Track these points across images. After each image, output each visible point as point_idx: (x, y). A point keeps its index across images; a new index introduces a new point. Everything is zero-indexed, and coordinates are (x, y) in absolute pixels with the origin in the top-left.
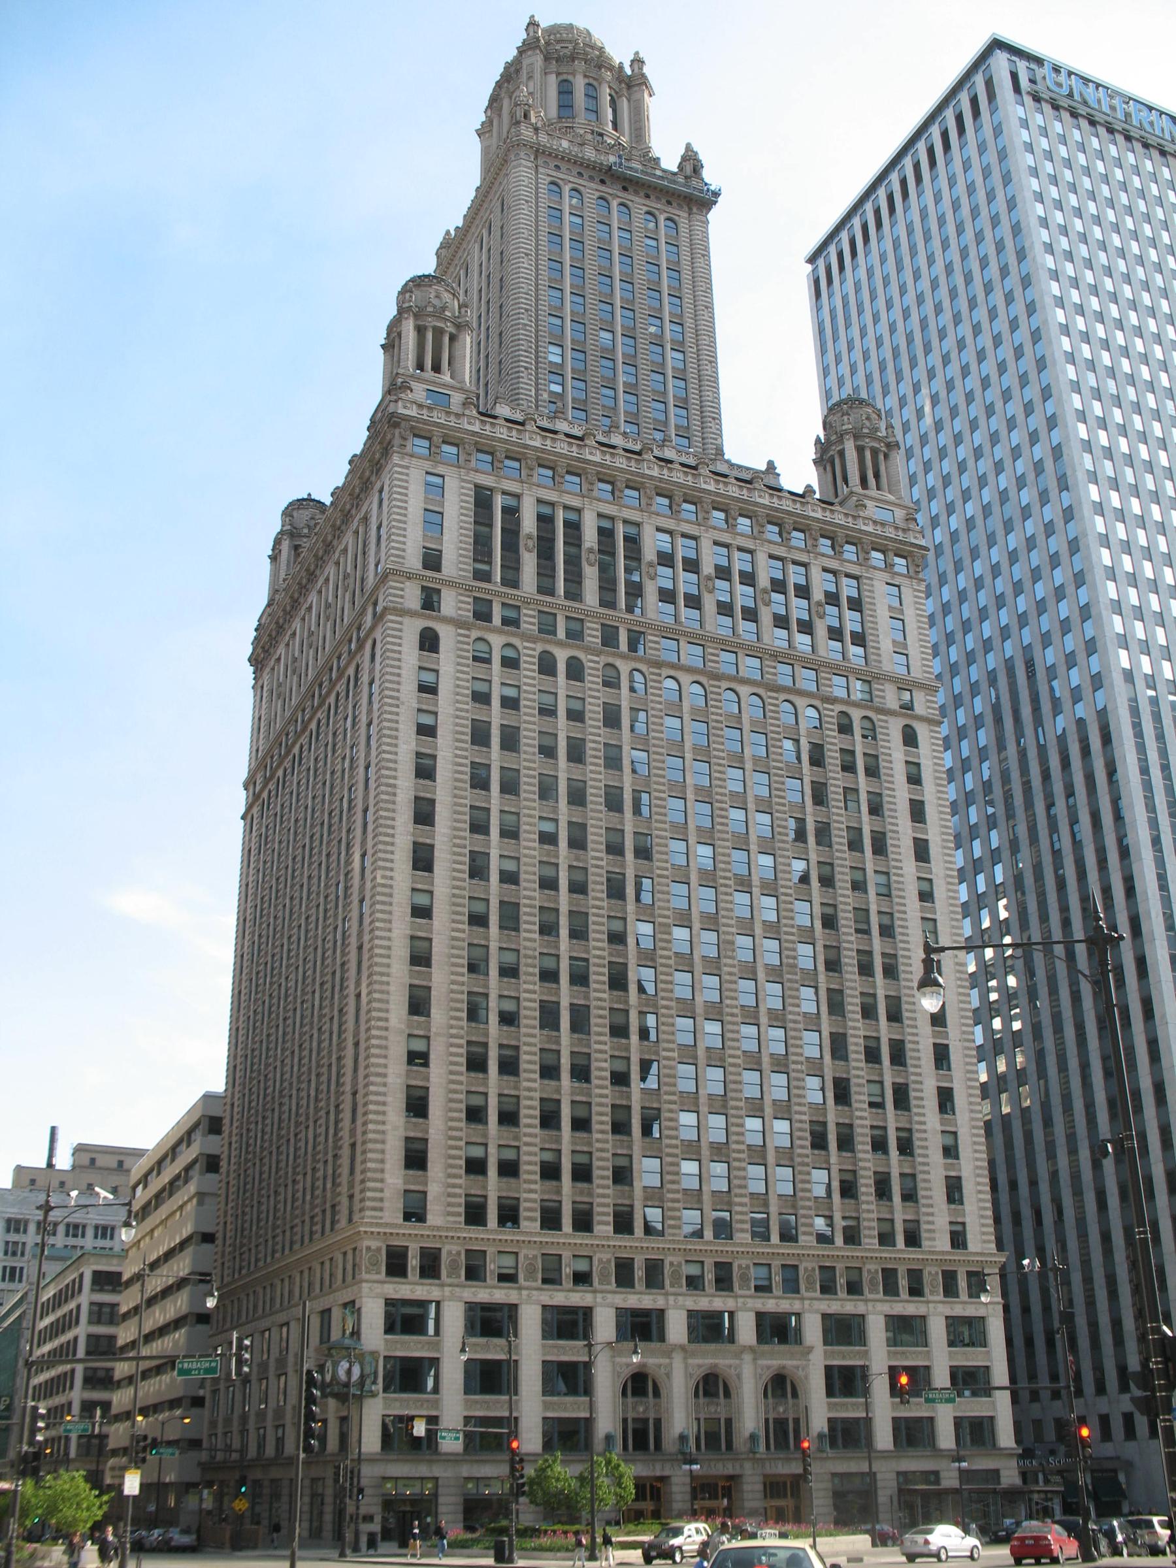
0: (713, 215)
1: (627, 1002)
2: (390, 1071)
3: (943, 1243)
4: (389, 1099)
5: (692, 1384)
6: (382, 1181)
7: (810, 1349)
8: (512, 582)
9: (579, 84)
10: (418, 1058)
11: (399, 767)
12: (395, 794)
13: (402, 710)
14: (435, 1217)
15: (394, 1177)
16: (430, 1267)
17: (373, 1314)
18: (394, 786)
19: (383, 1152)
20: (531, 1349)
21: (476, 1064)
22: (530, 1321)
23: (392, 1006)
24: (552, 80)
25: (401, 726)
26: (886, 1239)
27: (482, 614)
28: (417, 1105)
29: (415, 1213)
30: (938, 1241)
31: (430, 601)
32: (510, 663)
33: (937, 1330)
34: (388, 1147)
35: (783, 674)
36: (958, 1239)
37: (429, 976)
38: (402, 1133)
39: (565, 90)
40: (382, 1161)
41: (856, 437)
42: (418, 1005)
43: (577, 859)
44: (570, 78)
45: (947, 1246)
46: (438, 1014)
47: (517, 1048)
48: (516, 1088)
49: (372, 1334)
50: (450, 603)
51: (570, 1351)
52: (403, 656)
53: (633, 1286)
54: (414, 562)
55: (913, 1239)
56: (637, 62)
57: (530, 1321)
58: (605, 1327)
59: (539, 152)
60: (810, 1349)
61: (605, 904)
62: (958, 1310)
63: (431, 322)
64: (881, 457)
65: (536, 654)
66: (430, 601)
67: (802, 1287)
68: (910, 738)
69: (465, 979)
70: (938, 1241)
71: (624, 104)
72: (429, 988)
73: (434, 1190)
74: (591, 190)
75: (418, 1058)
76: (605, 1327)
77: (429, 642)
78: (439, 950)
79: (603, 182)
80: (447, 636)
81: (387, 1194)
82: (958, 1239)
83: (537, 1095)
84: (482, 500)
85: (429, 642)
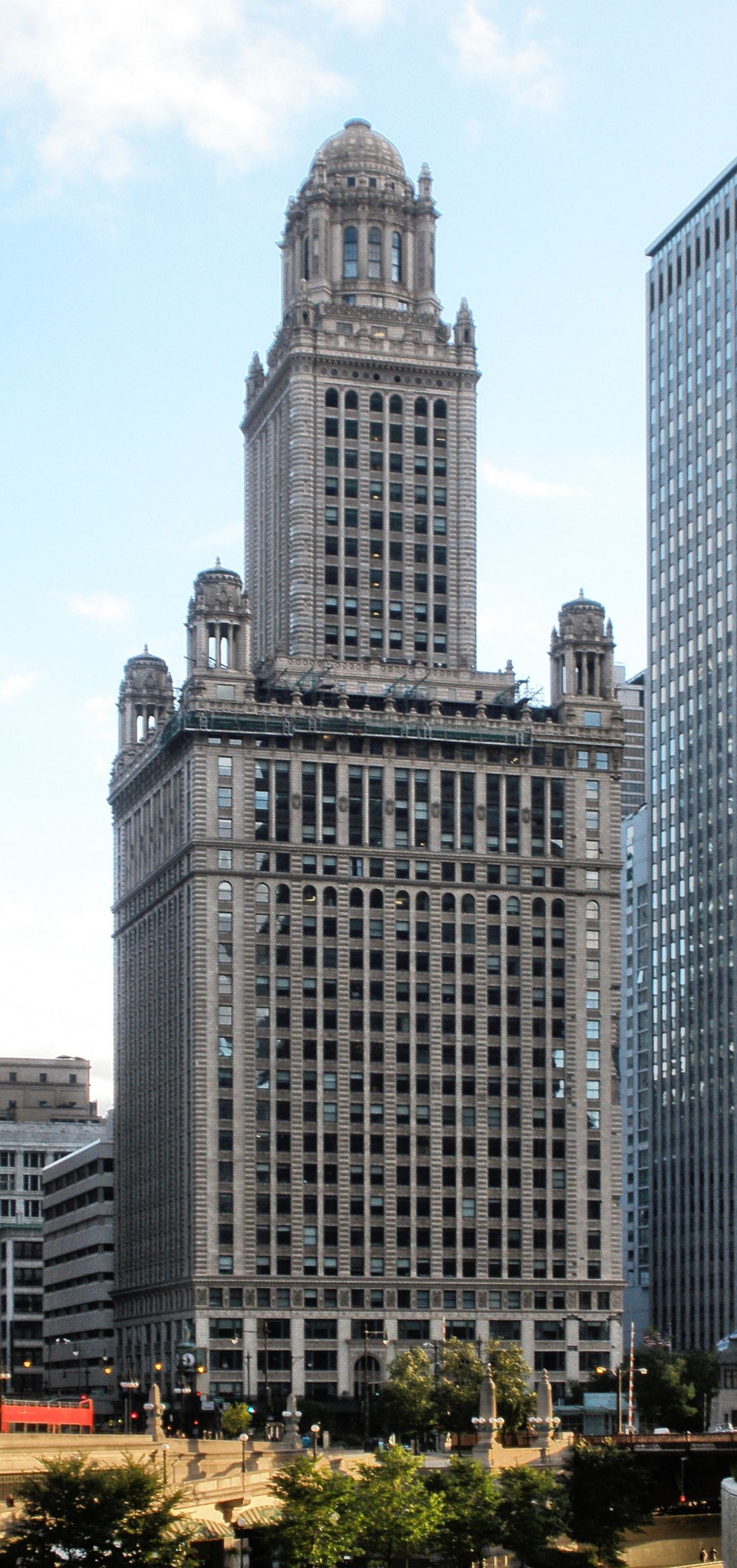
1: (362, 1130)
2: (208, 1186)
3: (582, 1275)
4: (208, 1203)
5: (353, 1364)
6: (205, 1251)
9: (363, 232)
11: (208, 987)
12: (205, 1006)
13: (208, 946)
16: (237, 1297)
17: (202, 1327)
18: (204, 1001)
19: (205, 1234)
20: (298, 1344)
22: (297, 1329)
23: (209, 1146)
24: (338, 230)
25: (208, 958)
26: (540, 1273)
34: (209, 1231)
36: (594, 1271)
37: (231, 1125)
38: (217, 1222)
39: (350, 238)
40: (205, 1240)
43: (330, 1036)
44: (355, 224)
45: (586, 1278)
46: (238, 1149)
47: (289, 1165)
48: (289, 1190)
49: (203, 1338)
51: (322, 1345)
52: (208, 907)
53: (363, 1306)
56: (426, 180)
57: (297, 1329)
58: (344, 1330)
61: (349, 1065)
64: (597, 660)
65: (301, 889)
67: (477, 1304)
69: (254, 1124)
71: (410, 239)
72: (231, 1132)
73: (238, 1254)
76: (344, 1330)
78: (237, 1106)
79: (377, 378)
81: (209, 1259)
82: (594, 1271)
83: (301, 1194)
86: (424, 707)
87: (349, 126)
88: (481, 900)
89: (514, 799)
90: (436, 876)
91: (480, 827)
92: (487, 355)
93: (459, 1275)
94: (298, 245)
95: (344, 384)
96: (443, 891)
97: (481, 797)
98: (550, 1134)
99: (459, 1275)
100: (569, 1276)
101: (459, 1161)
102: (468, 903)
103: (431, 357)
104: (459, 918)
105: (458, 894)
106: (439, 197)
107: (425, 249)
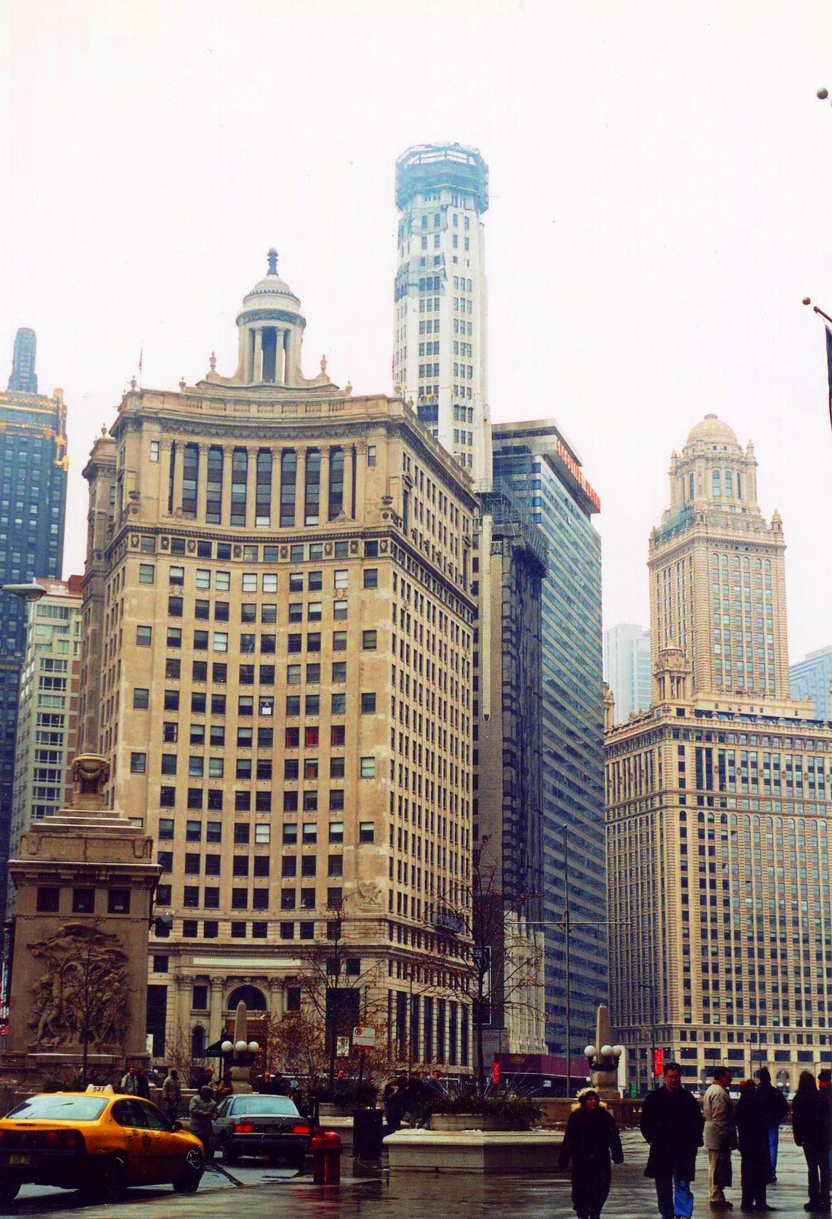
0: (786, 552)
8: (710, 786)
9: (723, 473)
10: (687, 970)
14: (694, 1023)
15: (681, 1009)
21: (705, 969)
24: (710, 472)
27: (700, 801)
28: (687, 984)
29: (688, 1021)
31: (683, 801)
32: (711, 821)
35: (810, 809)
39: (716, 476)
42: (686, 951)
46: (692, 955)
50: (691, 801)
54: (676, 785)
56: (750, 447)
59: (708, 540)
63: (676, 674)
66: (683, 801)
71: (744, 477)
73: (693, 1013)
74: (731, 552)
75: (687, 970)
77: (683, 816)
80: (688, 812)
84: (698, 751)
85: (683, 816)
87: (707, 417)
92: (789, 538)
94: (687, 478)
95: (721, 550)
103: (761, 538)
106: (759, 455)
107: (753, 481)
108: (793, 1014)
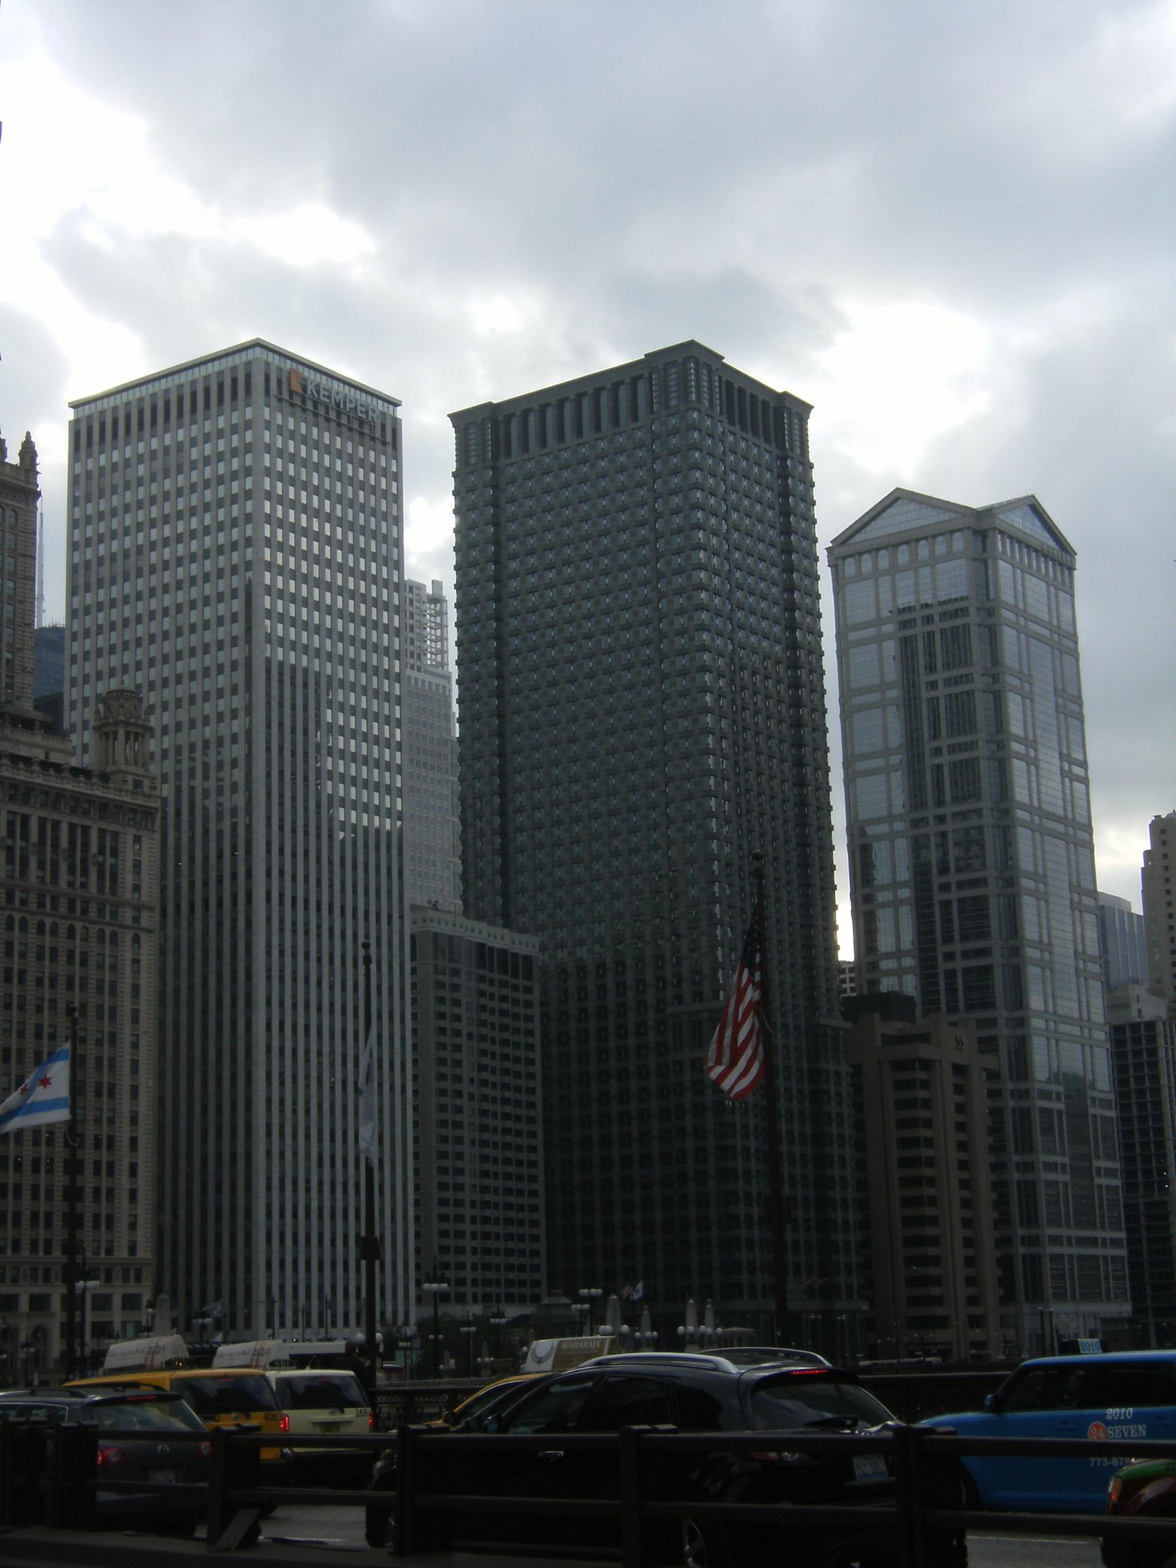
7: (53, 1314)
30: (122, 1253)
33: (117, 1301)
36: (132, 1249)
41: (126, 724)
55: (109, 1252)
60: (53, 1314)
62: (129, 1291)
68: (136, 940)
70: (122, 1253)
82: (132, 1249)
86: (27, 761)
88: (63, 926)
89: (86, 846)
90: (33, 906)
91: (63, 867)
93: (41, 1253)
96: (38, 918)
97: (64, 842)
98: (105, 1130)
99: (41, 1253)
100: (116, 1255)
101: (43, 1149)
102: (54, 931)
104: (48, 941)
105: (48, 921)
108: (26, 1234)
